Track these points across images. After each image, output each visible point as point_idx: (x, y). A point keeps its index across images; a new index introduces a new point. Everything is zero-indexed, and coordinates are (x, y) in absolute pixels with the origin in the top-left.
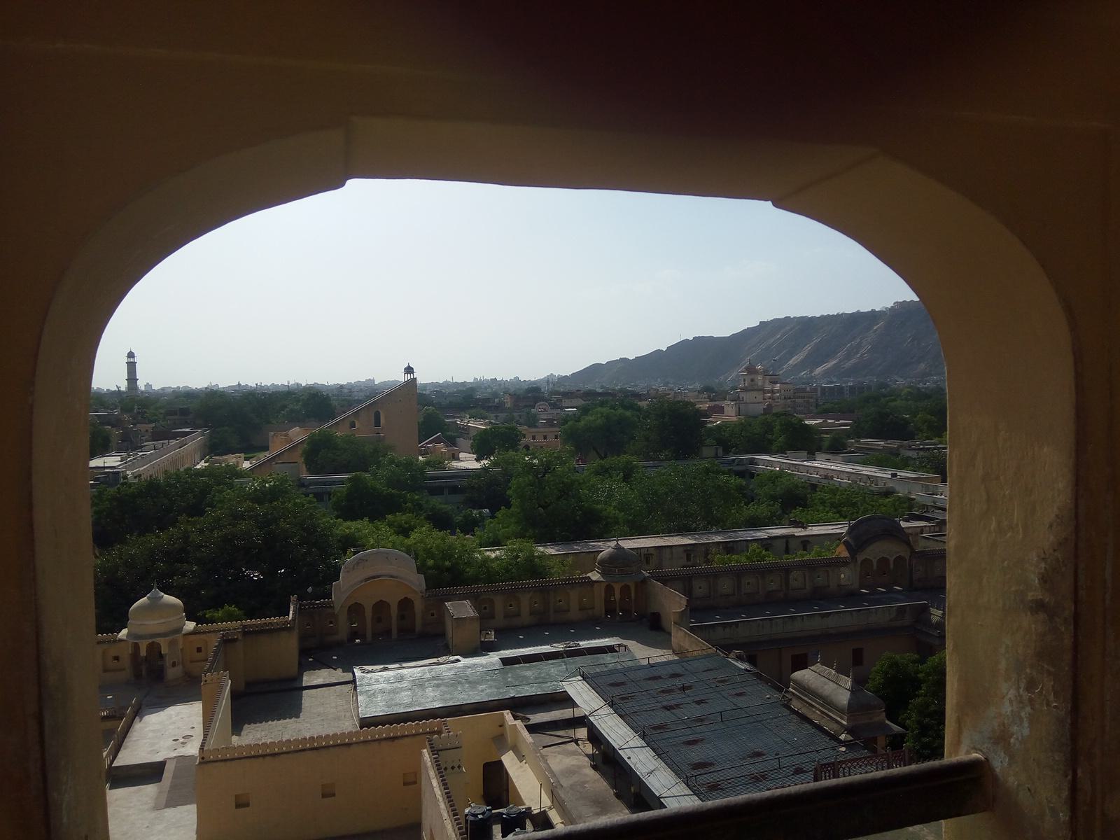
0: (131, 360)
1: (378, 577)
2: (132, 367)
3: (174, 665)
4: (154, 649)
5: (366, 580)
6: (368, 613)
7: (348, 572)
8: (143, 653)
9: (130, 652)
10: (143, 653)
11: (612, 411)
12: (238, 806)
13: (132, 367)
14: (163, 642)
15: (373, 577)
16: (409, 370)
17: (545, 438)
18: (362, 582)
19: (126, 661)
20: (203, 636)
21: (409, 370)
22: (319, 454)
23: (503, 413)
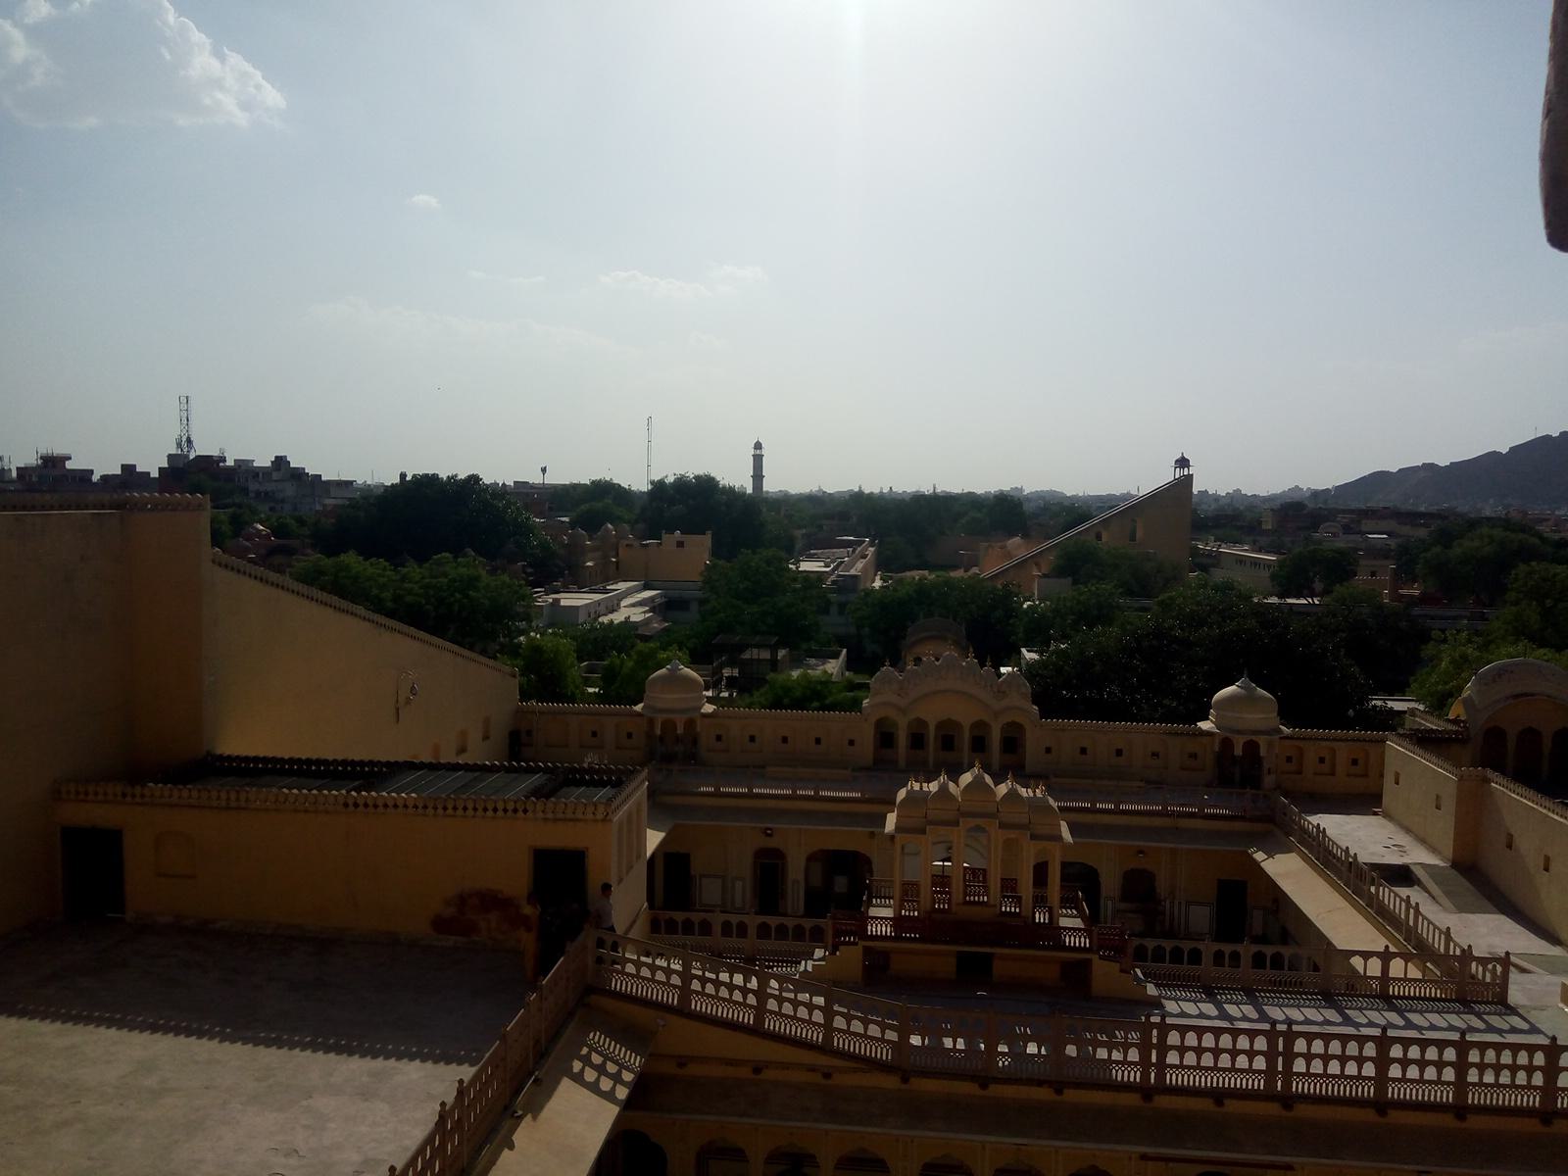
0: (758, 452)
1: (1532, 695)
2: (758, 460)
3: (1269, 773)
4: (1251, 747)
5: (1516, 696)
7: (1486, 684)
8: (1238, 751)
9: (1217, 750)
10: (1238, 751)
11: (1508, 533)
13: (758, 460)
14: (1262, 740)
15: (1526, 695)
16: (1183, 462)
17: (1373, 574)
18: (1507, 698)
20: (1297, 743)
21: (1183, 462)
22: (1075, 564)
23: (1306, 532)
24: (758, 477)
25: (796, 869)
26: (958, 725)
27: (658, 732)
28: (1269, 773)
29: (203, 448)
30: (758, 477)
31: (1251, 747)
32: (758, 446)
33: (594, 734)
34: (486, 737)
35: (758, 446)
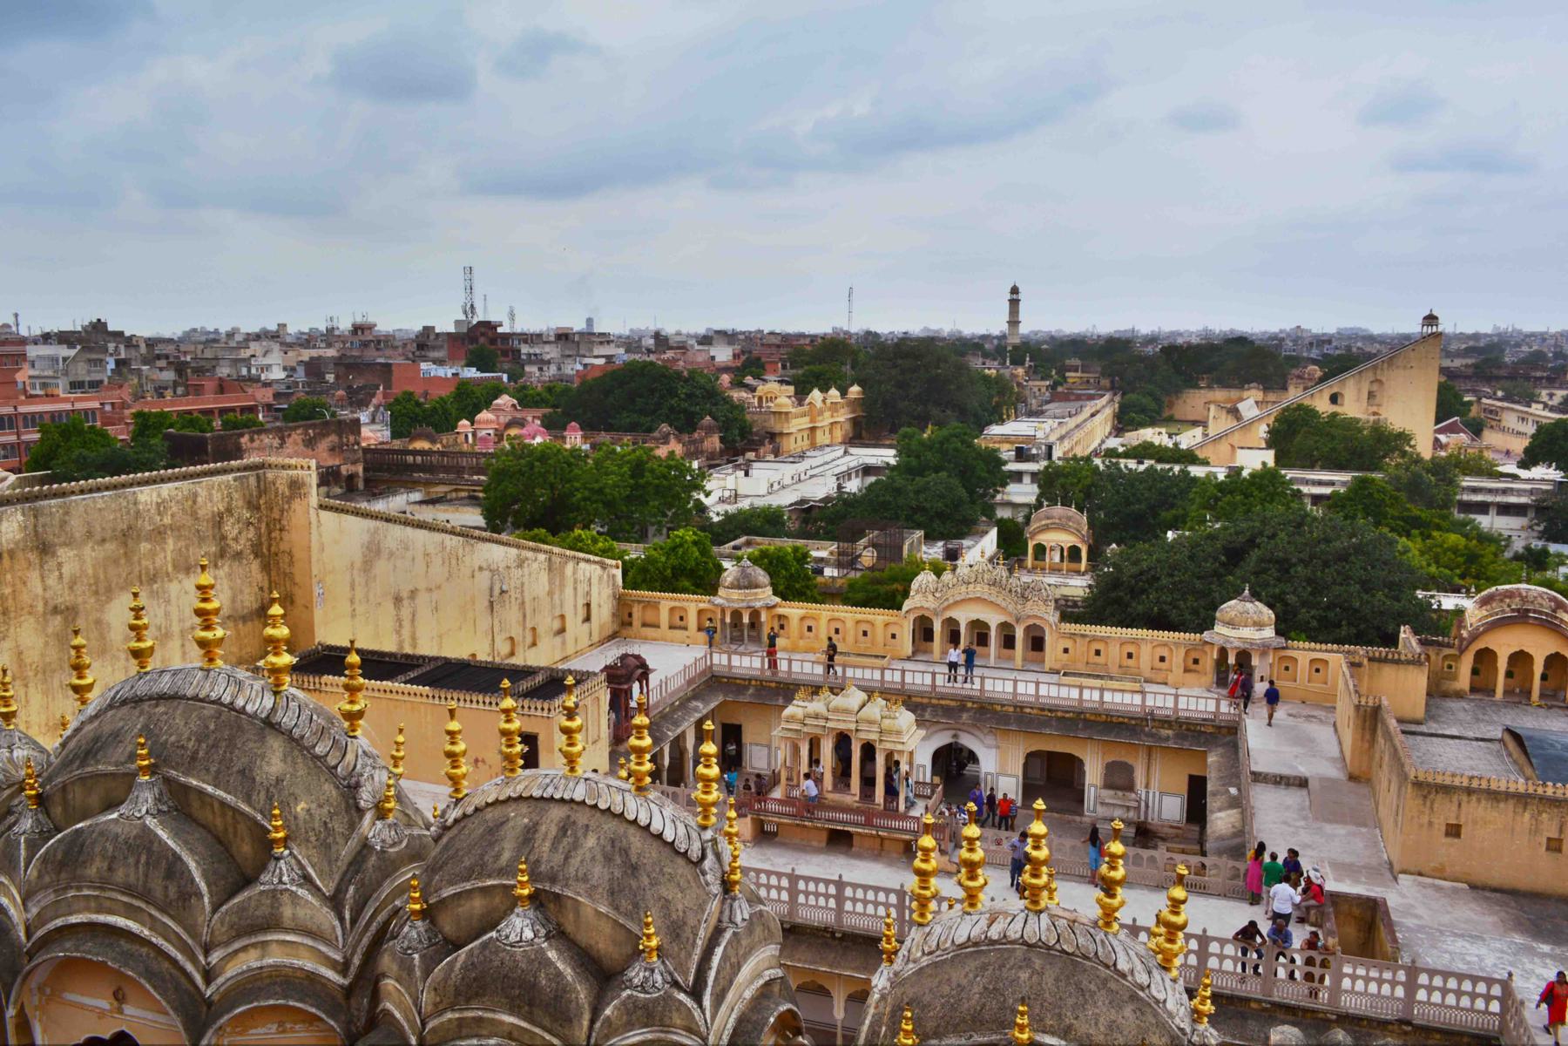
2: (1014, 303)
3: (1262, 679)
4: (1244, 656)
6: (1502, 665)
12: (1458, 835)
13: (1014, 303)
16: (1431, 319)
21: (1431, 319)
24: (1014, 322)
26: (986, 626)
27: (728, 620)
28: (1262, 679)
29: (480, 316)
30: (1014, 322)
31: (1244, 656)
32: (1015, 290)
33: (681, 618)
34: (588, 619)
35: (1015, 290)
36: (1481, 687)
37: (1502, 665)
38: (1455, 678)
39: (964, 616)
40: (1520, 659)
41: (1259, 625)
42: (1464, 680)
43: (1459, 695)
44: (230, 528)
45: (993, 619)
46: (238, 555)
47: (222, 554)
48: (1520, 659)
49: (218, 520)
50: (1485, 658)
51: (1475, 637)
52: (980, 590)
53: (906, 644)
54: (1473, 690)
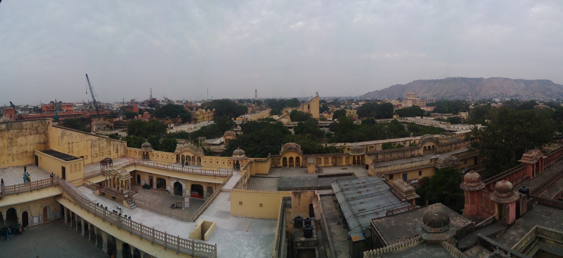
6: (288, 160)
19: (232, 164)
25: (155, 181)
36: (285, 165)
37: (288, 160)
38: (279, 163)
39: (186, 154)
40: (291, 158)
41: (240, 154)
42: (281, 164)
43: (280, 167)
44: (39, 129)
45: (191, 155)
46: (40, 133)
47: (37, 133)
48: (291, 158)
49: (37, 128)
50: (285, 159)
51: (282, 155)
52: (188, 149)
53: (175, 160)
54: (283, 165)
